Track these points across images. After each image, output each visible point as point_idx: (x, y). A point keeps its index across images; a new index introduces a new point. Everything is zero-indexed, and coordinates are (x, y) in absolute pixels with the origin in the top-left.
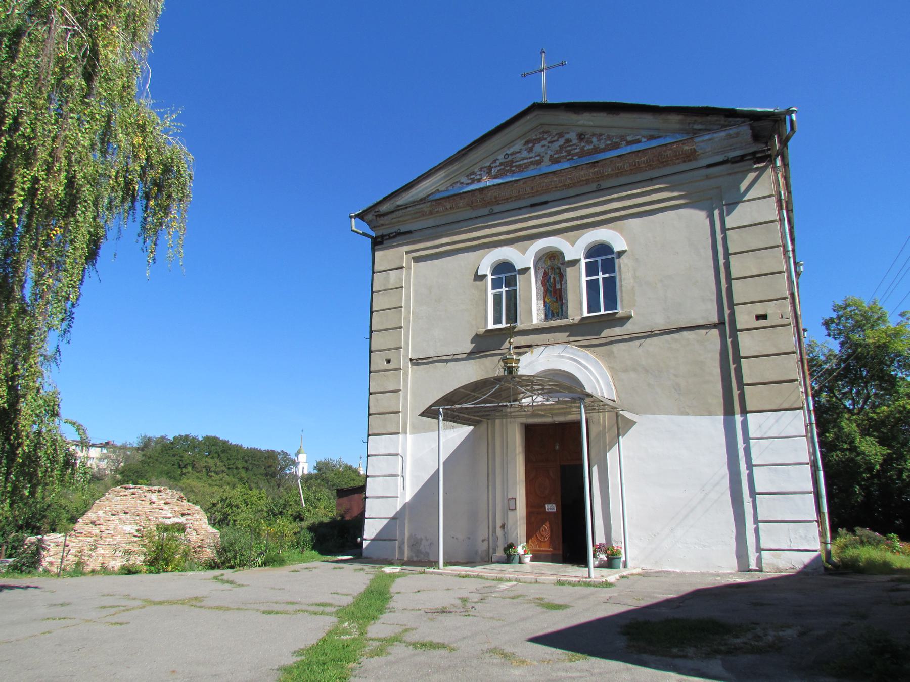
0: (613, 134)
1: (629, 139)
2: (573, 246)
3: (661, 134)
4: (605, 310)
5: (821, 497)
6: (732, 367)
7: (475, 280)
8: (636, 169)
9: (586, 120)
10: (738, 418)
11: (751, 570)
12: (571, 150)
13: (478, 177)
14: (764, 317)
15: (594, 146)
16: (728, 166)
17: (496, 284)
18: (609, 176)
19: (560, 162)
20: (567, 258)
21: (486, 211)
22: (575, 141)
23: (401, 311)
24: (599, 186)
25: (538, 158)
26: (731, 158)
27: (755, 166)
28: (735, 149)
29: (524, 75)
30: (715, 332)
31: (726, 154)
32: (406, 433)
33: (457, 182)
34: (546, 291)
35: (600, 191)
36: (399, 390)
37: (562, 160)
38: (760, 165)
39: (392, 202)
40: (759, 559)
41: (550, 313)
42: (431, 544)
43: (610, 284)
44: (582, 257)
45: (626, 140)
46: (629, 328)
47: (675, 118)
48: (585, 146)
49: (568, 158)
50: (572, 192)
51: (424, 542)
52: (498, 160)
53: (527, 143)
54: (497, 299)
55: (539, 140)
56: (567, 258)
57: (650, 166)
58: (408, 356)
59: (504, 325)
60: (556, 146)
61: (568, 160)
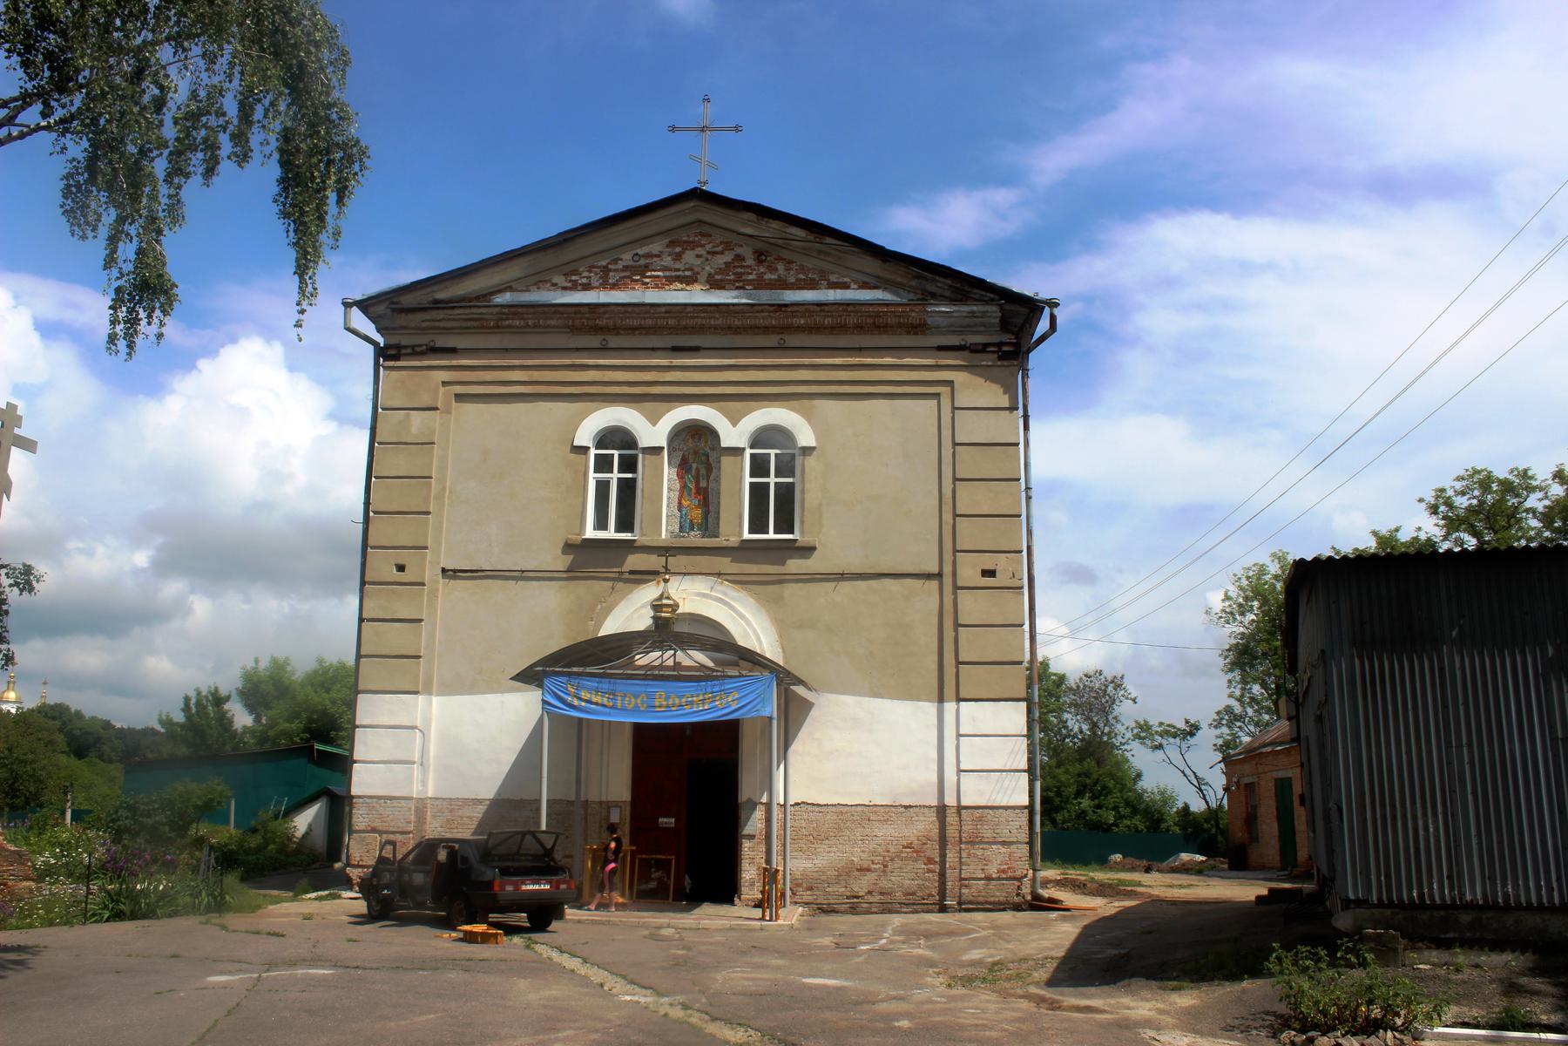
0: (811, 267)
1: (833, 278)
2: (734, 425)
4: (776, 532)
5: (1035, 814)
12: (742, 274)
13: (584, 281)
14: (988, 573)
15: (779, 276)
17: (603, 464)
18: (799, 329)
20: (724, 444)
21: (594, 341)
22: (750, 262)
24: (782, 342)
25: (687, 273)
26: (971, 344)
29: (673, 129)
35: (782, 349)
37: (727, 287)
39: (428, 290)
43: (786, 496)
45: (828, 280)
48: (765, 274)
49: (737, 284)
50: (739, 340)
52: (621, 259)
53: (672, 243)
54: (602, 488)
55: (693, 245)
56: (724, 444)
58: (438, 564)
59: (611, 533)
60: (721, 260)
61: (738, 288)
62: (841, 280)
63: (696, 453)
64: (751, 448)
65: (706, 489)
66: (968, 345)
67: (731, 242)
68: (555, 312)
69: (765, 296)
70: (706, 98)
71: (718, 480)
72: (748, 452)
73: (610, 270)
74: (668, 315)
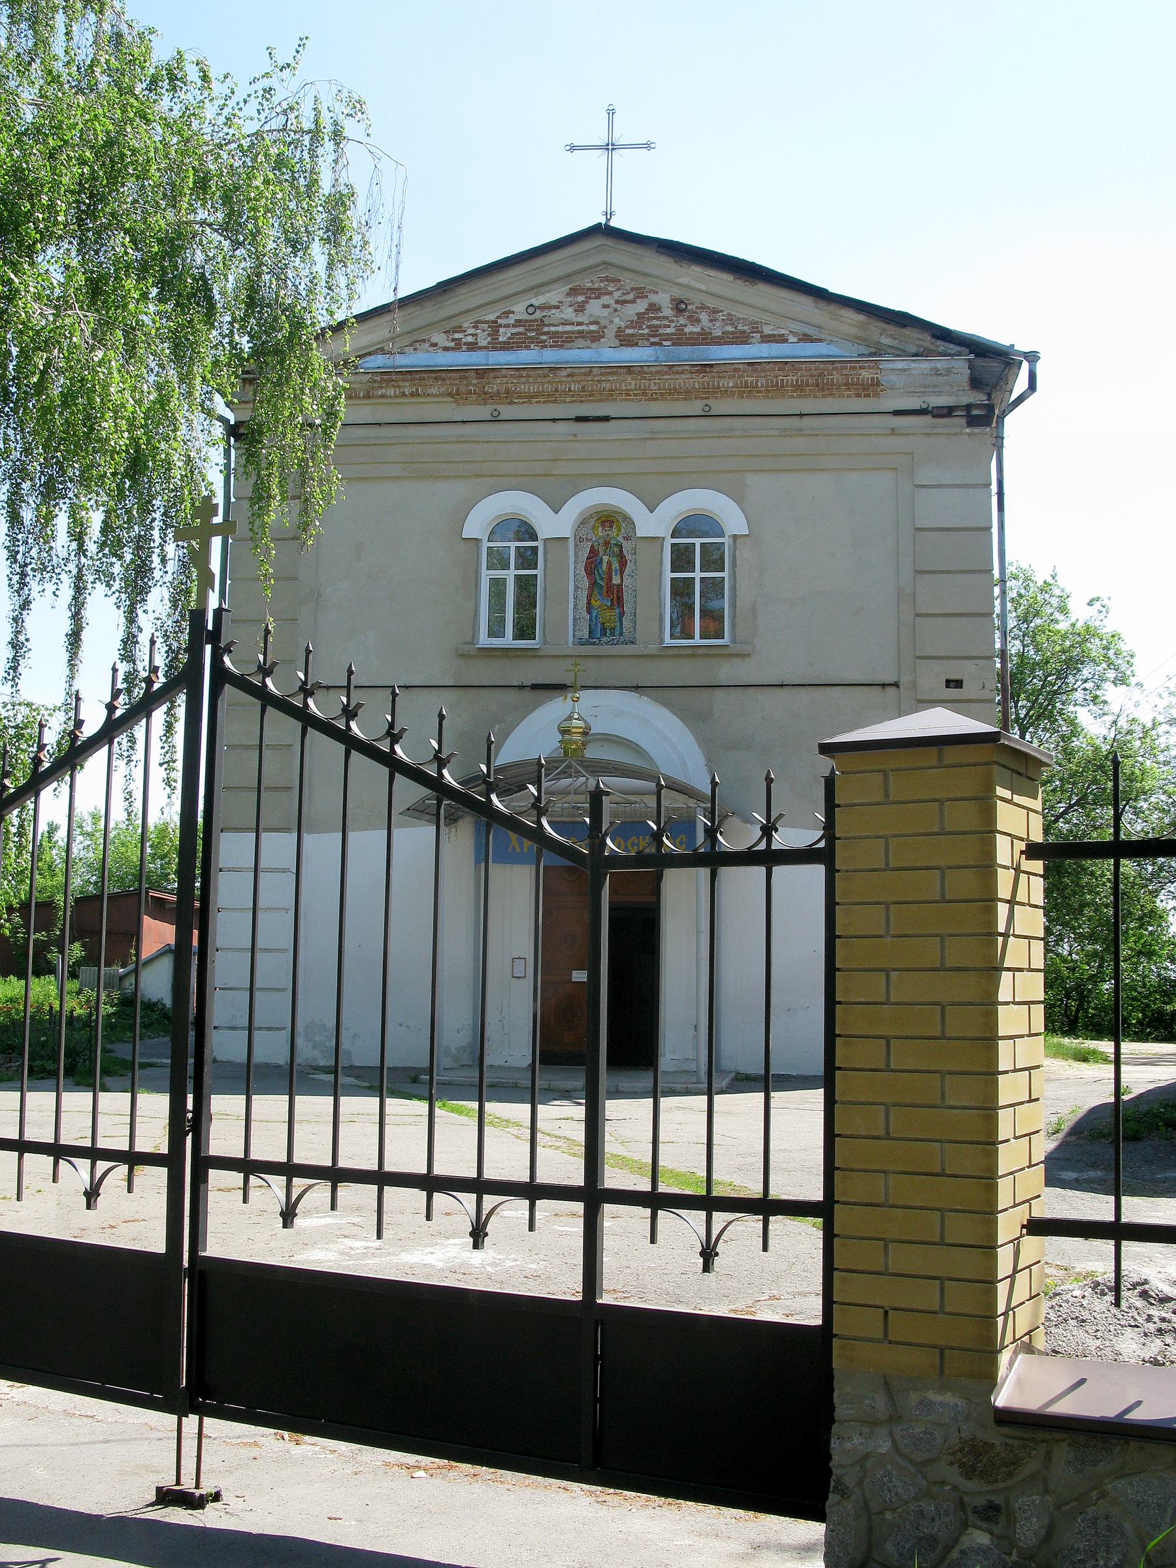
1: (767, 330)
3: (823, 336)
4: (701, 638)
8: (776, 390)
9: (693, 276)
13: (470, 339)
14: (958, 684)
15: (702, 329)
16: (927, 420)
18: (727, 393)
19: (636, 344)
21: (485, 412)
22: (667, 312)
24: (707, 409)
25: (593, 327)
28: (940, 394)
29: (573, 148)
31: (925, 398)
33: (424, 341)
37: (640, 343)
42: (354, 1036)
48: (686, 326)
49: (652, 340)
52: (513, 312)
53: (573, 292)
54: (498, 586)
55: (598, 293)
57: (800, 389)
59: (508, 640)
60: (632, 311)
61: (653, 344)
62: (775, 332)
63: (607, 543)
64: (673, 536)
65: (620, 586)
66: (930, 409)
67: (644, 288)
68: (436, 379)
69: (686, 353)
70: (611, 108)
72: (670, 541)
73: (501, 326)
74: (570, 379)
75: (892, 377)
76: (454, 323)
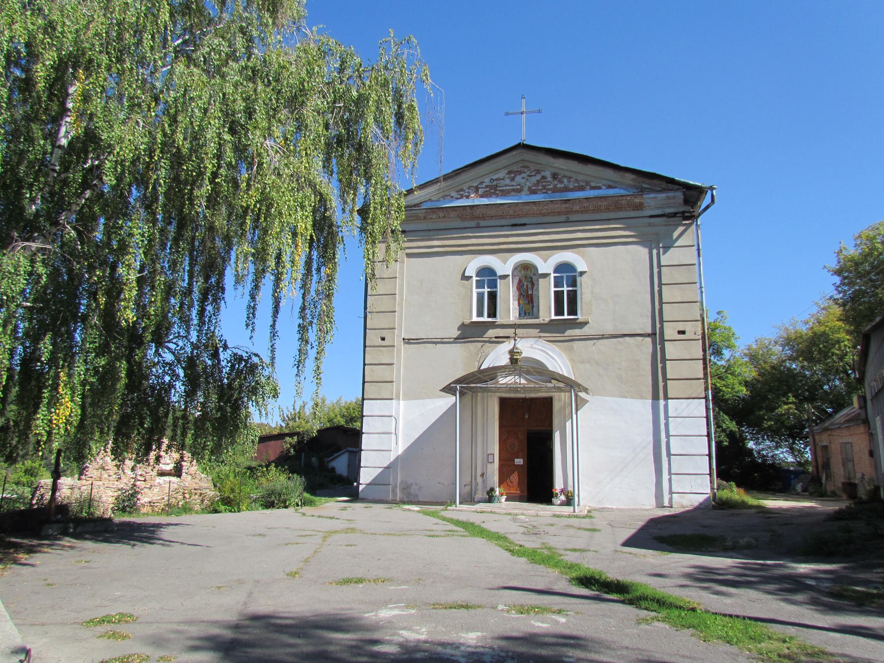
1: (593, 184)
4: (569, 314)
6: (660, 366)
7: (462, 279)
8: (597, 210)
9: (560, 164)
10: (662, 402)
11: (665, 507)
12: (546, 185)
13: (467, 194)
14: (683, 332)
16: (664, 219)
17: (480, 285)
18: (576, 212)
20: (540, 272)
21: (473, 224)
22: (549, 179)
23: (396, 298)
25: (518, 187)
27: (684, 222)
28: (670, 207)
29: (507, 114)
30: (649, 340)
32: (399, 399)
33: (447, 195)
34: (520, 295)
35: (567, 222)
36: (393, 364)
38: (687, 222)
40: (671, 500)
41: (523, 313)
43: (573, 297)
44: (552, 272)
46: (586, 331)
47: (629, 176)
51: (414, 487)
53: (510, 172)
54: (480, 297)
55: (520, 173)
56: (540, 272)
57: (608, 209)
59: (485, 319)
60: (534, 180)
65: (532, 295)
69: (558, 197)
71: (538, 290)
72: (553, 275)
75: (648, 201)
76: (460, 187)
